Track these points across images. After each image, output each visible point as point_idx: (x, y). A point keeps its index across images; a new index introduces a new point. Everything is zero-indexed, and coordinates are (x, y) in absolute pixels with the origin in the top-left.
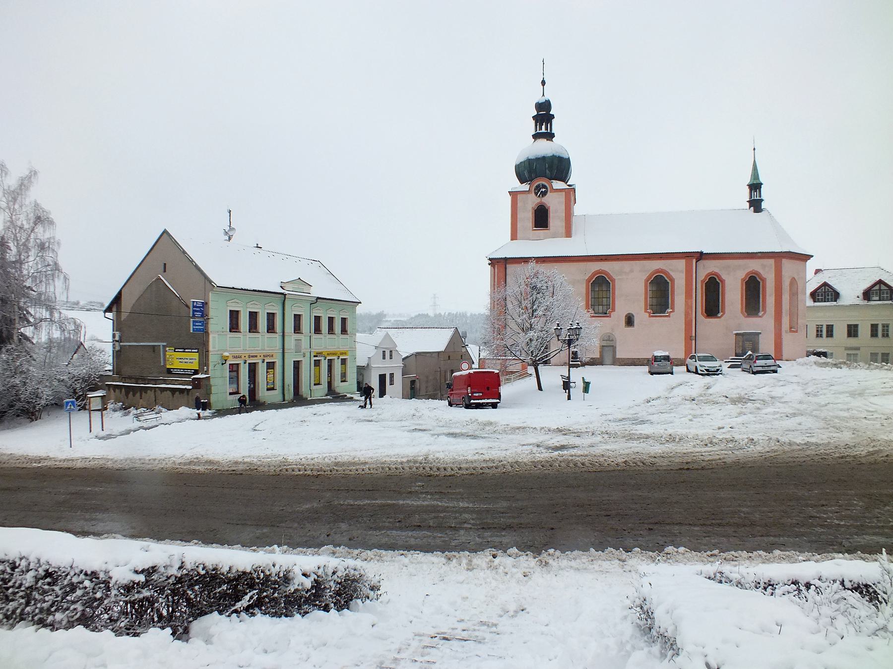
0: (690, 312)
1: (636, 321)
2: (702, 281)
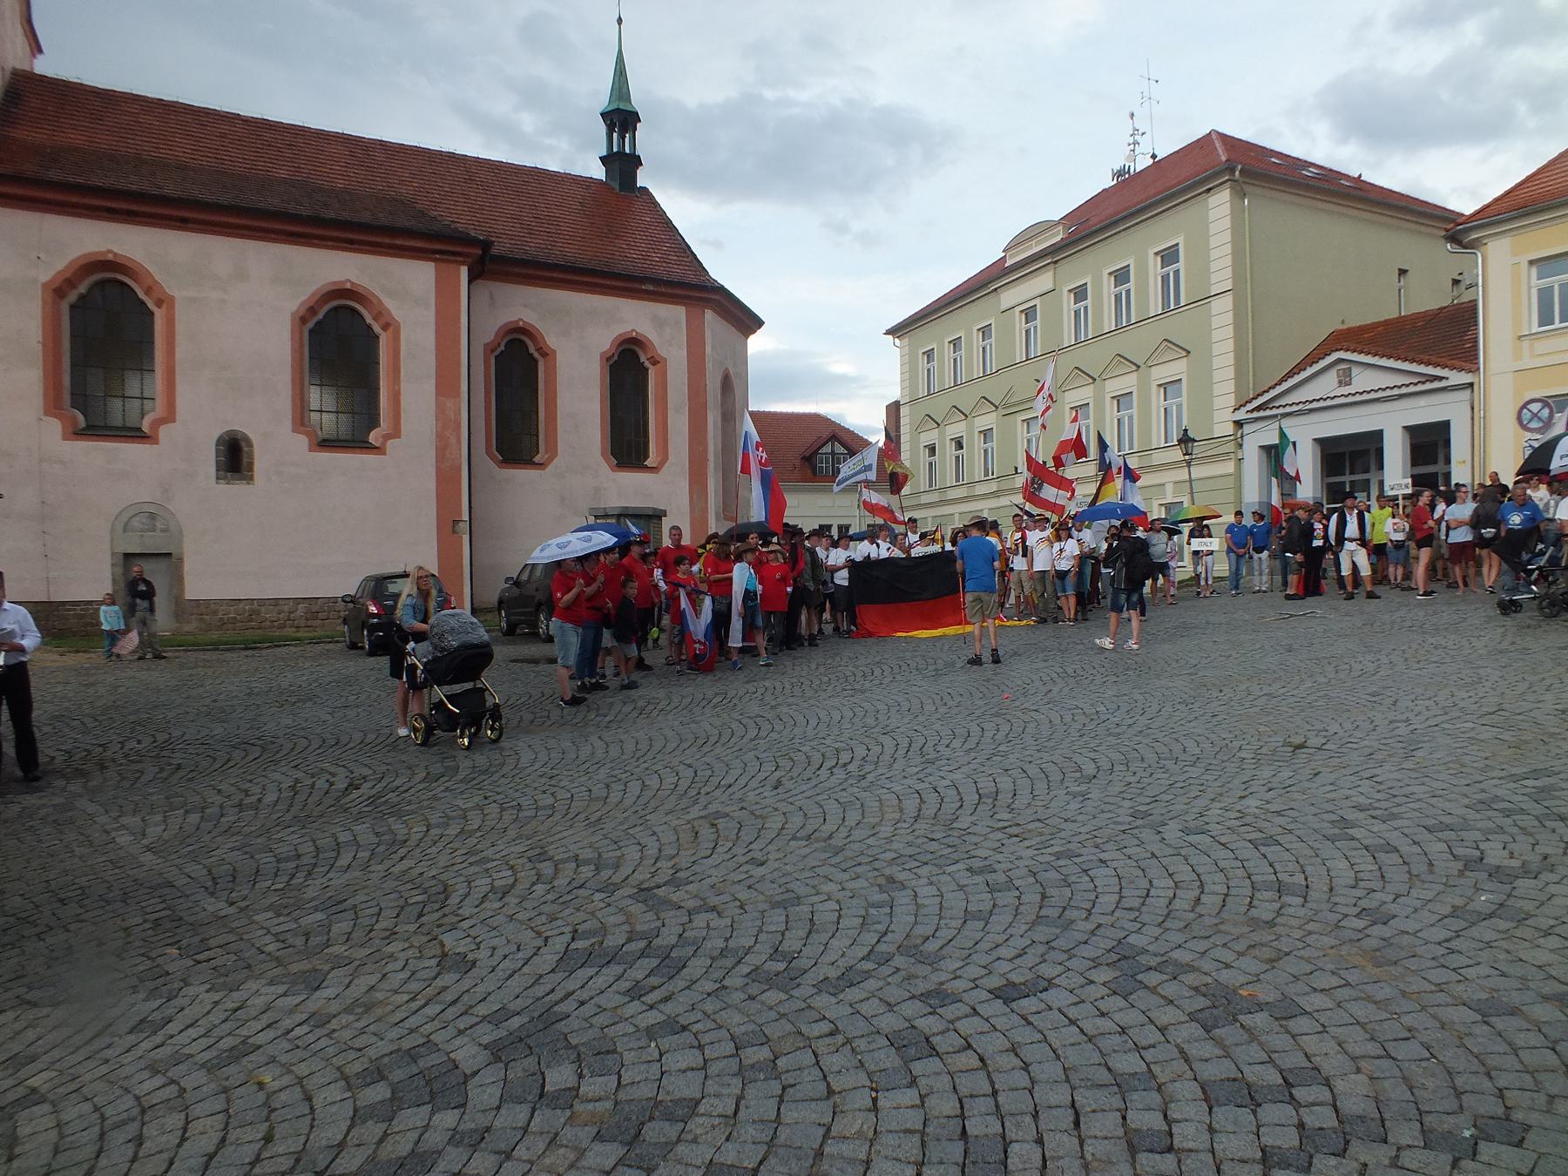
0: (453, 440)
1: (262, 461)
2: (486, 345)
